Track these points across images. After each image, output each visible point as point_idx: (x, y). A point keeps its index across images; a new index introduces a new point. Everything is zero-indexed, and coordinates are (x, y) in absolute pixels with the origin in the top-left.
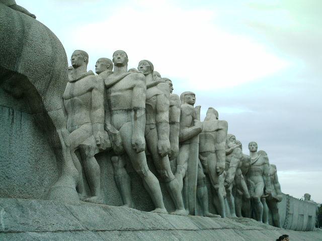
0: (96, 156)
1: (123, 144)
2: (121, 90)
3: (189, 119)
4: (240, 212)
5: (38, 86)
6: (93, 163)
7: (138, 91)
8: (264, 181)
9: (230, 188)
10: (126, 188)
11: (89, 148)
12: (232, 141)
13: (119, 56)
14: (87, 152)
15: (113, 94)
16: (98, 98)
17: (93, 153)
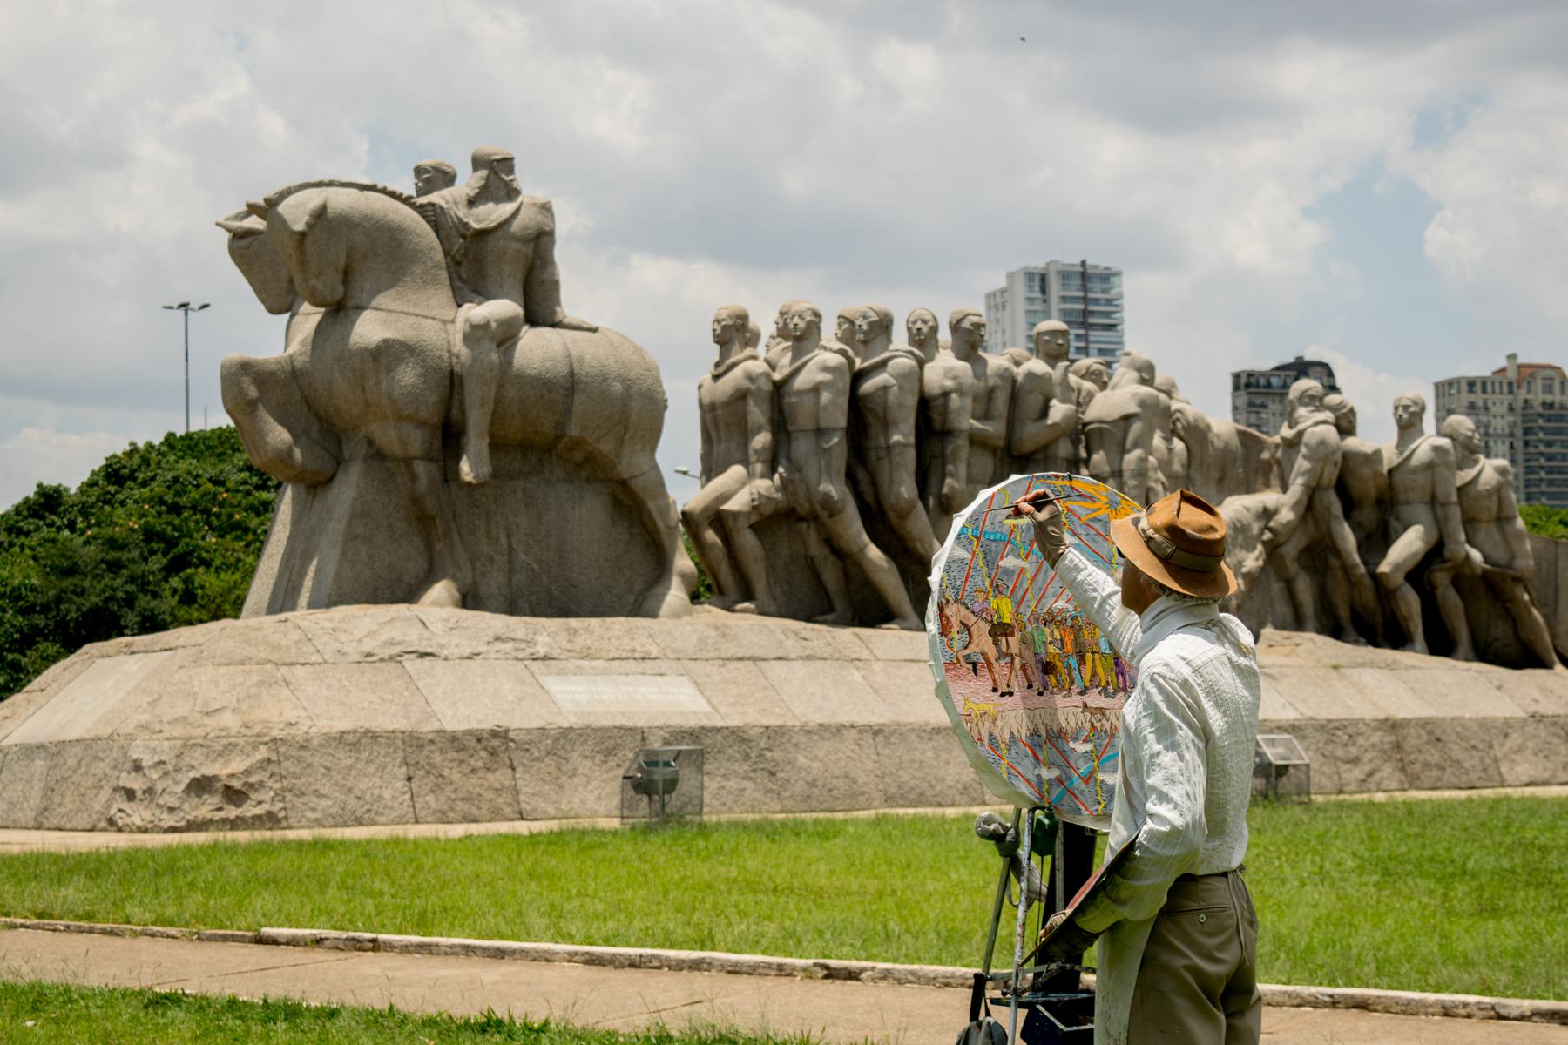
0: (752, 527)
1: (810, 502)
2: (800, 393)
3: (1034, 402)
4: (1344, 613)
5: (606, 447)
6: (748, 542)
7: (825, 397)
8: (1436, 519)
9: (1290, 550)
10: (831, 576)
11: (735, 515)
12: (1306, 405)
13: (796, 320)
14: (730, 523)
15: (787, 400)
16: (757, 413)
17: (743, 523)
